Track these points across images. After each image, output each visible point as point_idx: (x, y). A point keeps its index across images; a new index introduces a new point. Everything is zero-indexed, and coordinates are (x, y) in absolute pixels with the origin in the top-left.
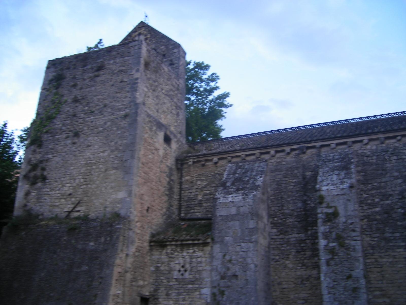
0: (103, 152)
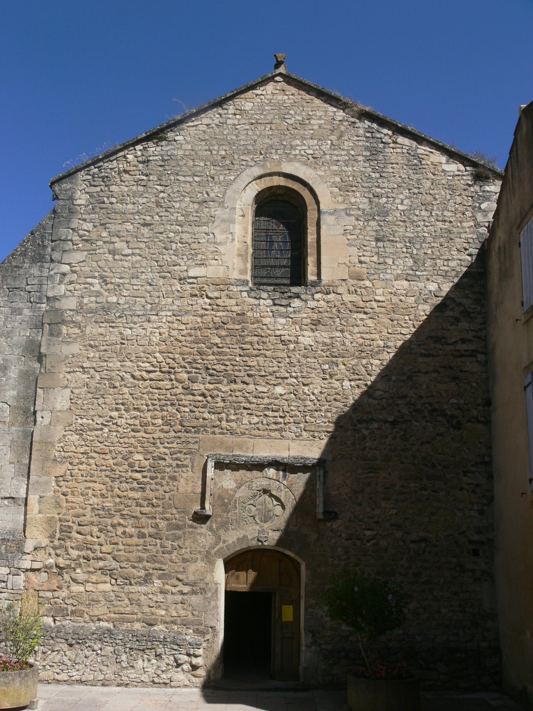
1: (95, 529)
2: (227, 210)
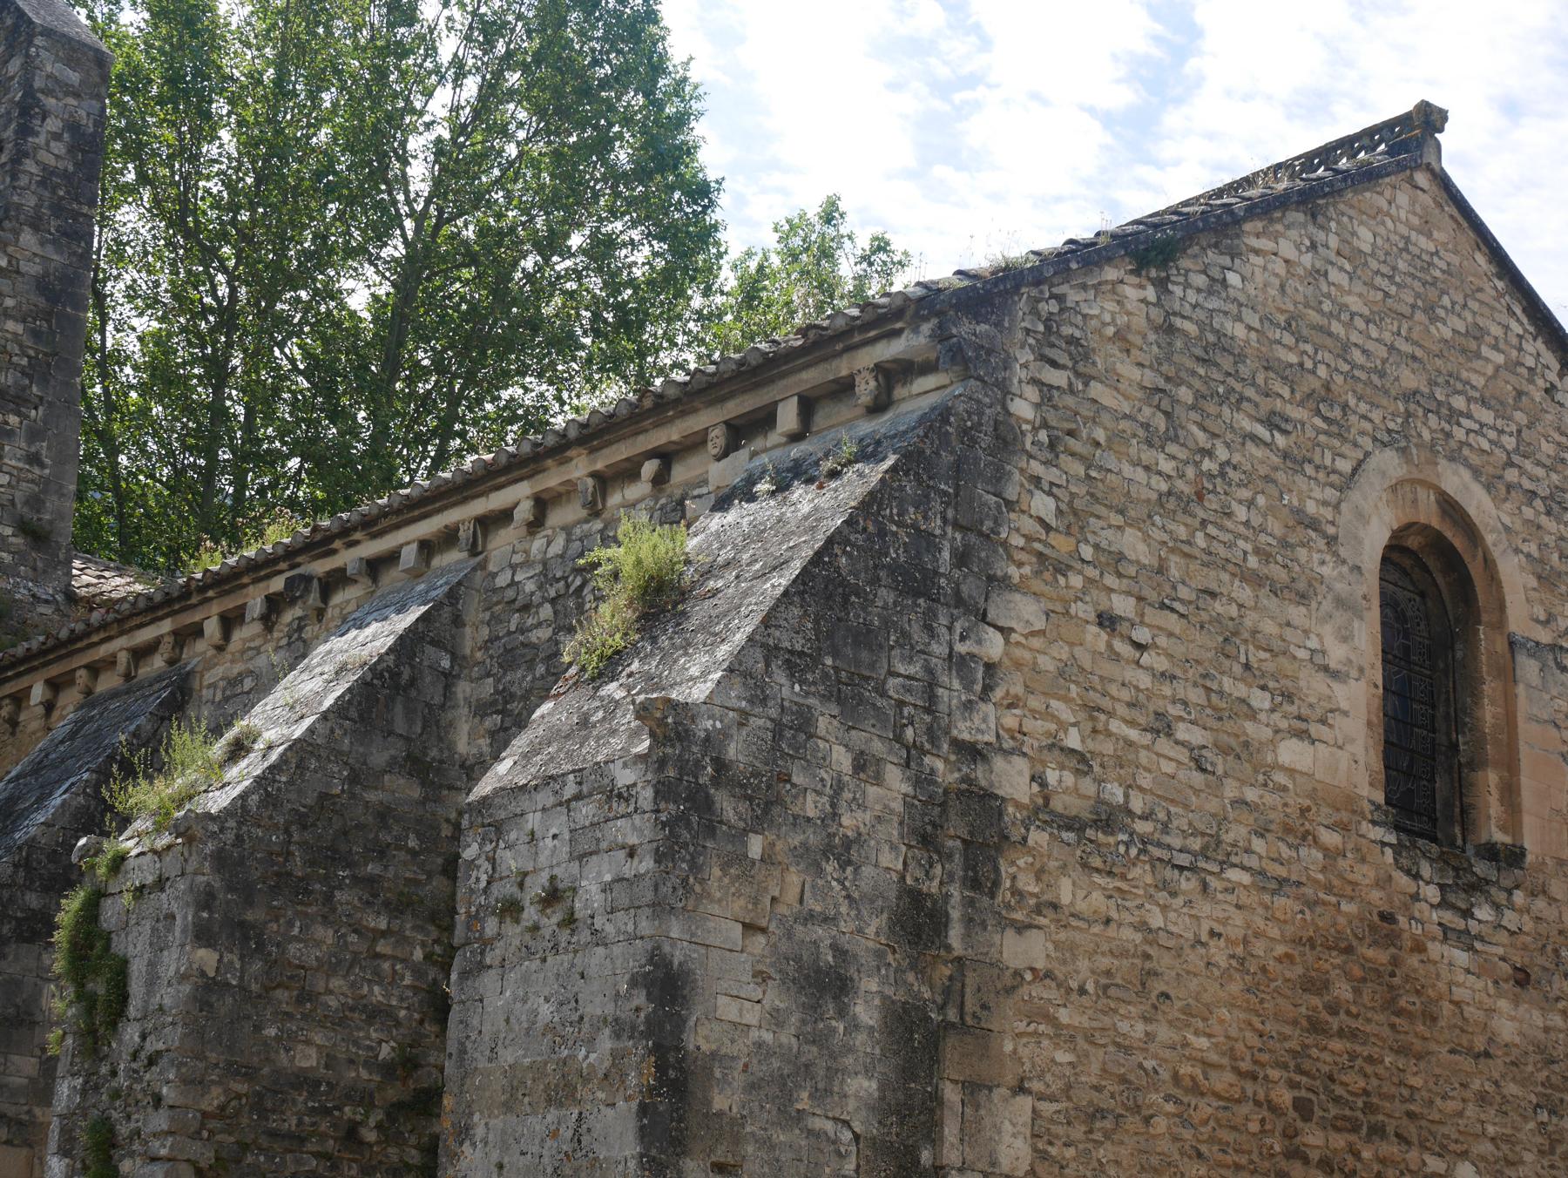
2: (1345, 569)
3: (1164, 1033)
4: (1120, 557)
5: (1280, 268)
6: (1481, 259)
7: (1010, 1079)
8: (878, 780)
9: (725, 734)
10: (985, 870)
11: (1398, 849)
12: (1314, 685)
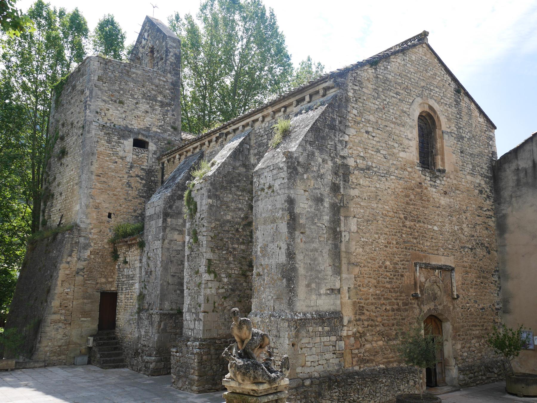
0: (72, 170)
1: (373, 307)
3: (380, 206)
4: (369, 120)
5: (398, 64)
6: (436, 60)
7: (353, 215)
8: (327, 163)
9: (299, 157)
10: (347, 178)
11: (422, 171)
12: (406, 142)
